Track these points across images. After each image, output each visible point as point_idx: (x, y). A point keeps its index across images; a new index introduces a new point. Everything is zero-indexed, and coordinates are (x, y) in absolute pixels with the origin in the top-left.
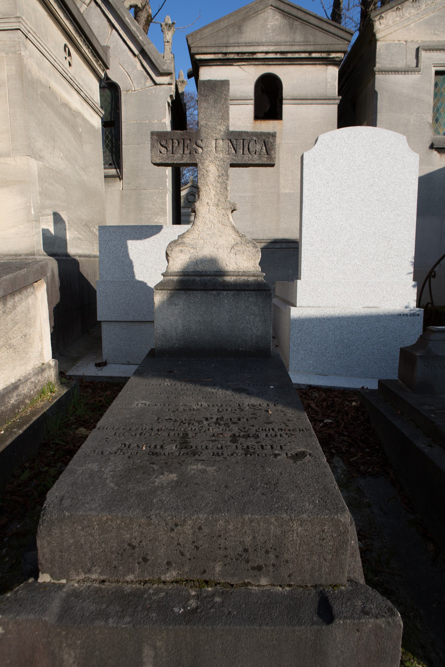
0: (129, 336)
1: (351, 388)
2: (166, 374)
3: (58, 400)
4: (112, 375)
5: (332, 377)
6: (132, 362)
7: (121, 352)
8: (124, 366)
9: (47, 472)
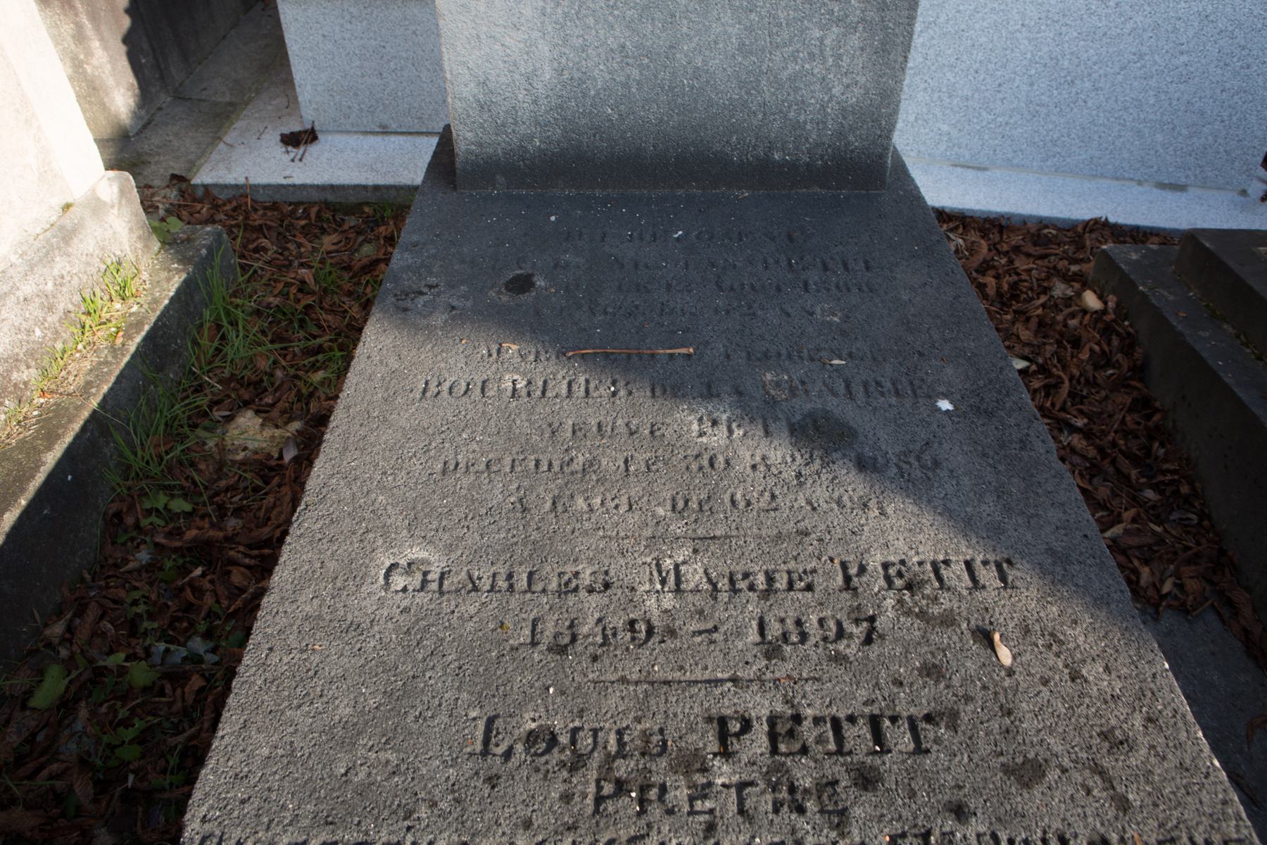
0: (373, 42)
1: (1058, 219)
2: (505, 299)
3: (148, 333)
4: (335, 181)
5: (998, 173)
6: (394, 127)
7: (356, 94)
8: (372, 140)
9: (122, 671)
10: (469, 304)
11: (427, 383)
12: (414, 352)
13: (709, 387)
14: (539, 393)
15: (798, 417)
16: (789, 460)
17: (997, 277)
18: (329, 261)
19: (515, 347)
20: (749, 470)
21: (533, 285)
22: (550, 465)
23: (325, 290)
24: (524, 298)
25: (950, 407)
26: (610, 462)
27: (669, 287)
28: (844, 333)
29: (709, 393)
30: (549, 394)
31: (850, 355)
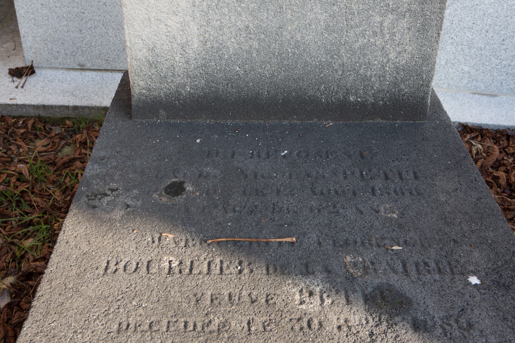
0: (76, 10)
2: (164, 200)
4: (46, 103)
5: (505, 98)
6: (89, 65)
7: (63, 44)
8: (73, 73)
10: (139, 203)
11: (108, 262)
12: (100, 239)
13: (307, 266)
14: (187, 271)
15: (370, 290)
16: (364, 322)
17: (507, 172)
18: (40, 159)
19: (171, 236)
20: (336, 330)
21: (184, 189)
22: (195, 325)
23: (36, 180)
24: (179, 199)
25: (478, 282)
26: (238, 324)
27: (278, 191)
28: (401, 226)
29: (307, 272)
30: (195, 272)
31: (405, 242)
